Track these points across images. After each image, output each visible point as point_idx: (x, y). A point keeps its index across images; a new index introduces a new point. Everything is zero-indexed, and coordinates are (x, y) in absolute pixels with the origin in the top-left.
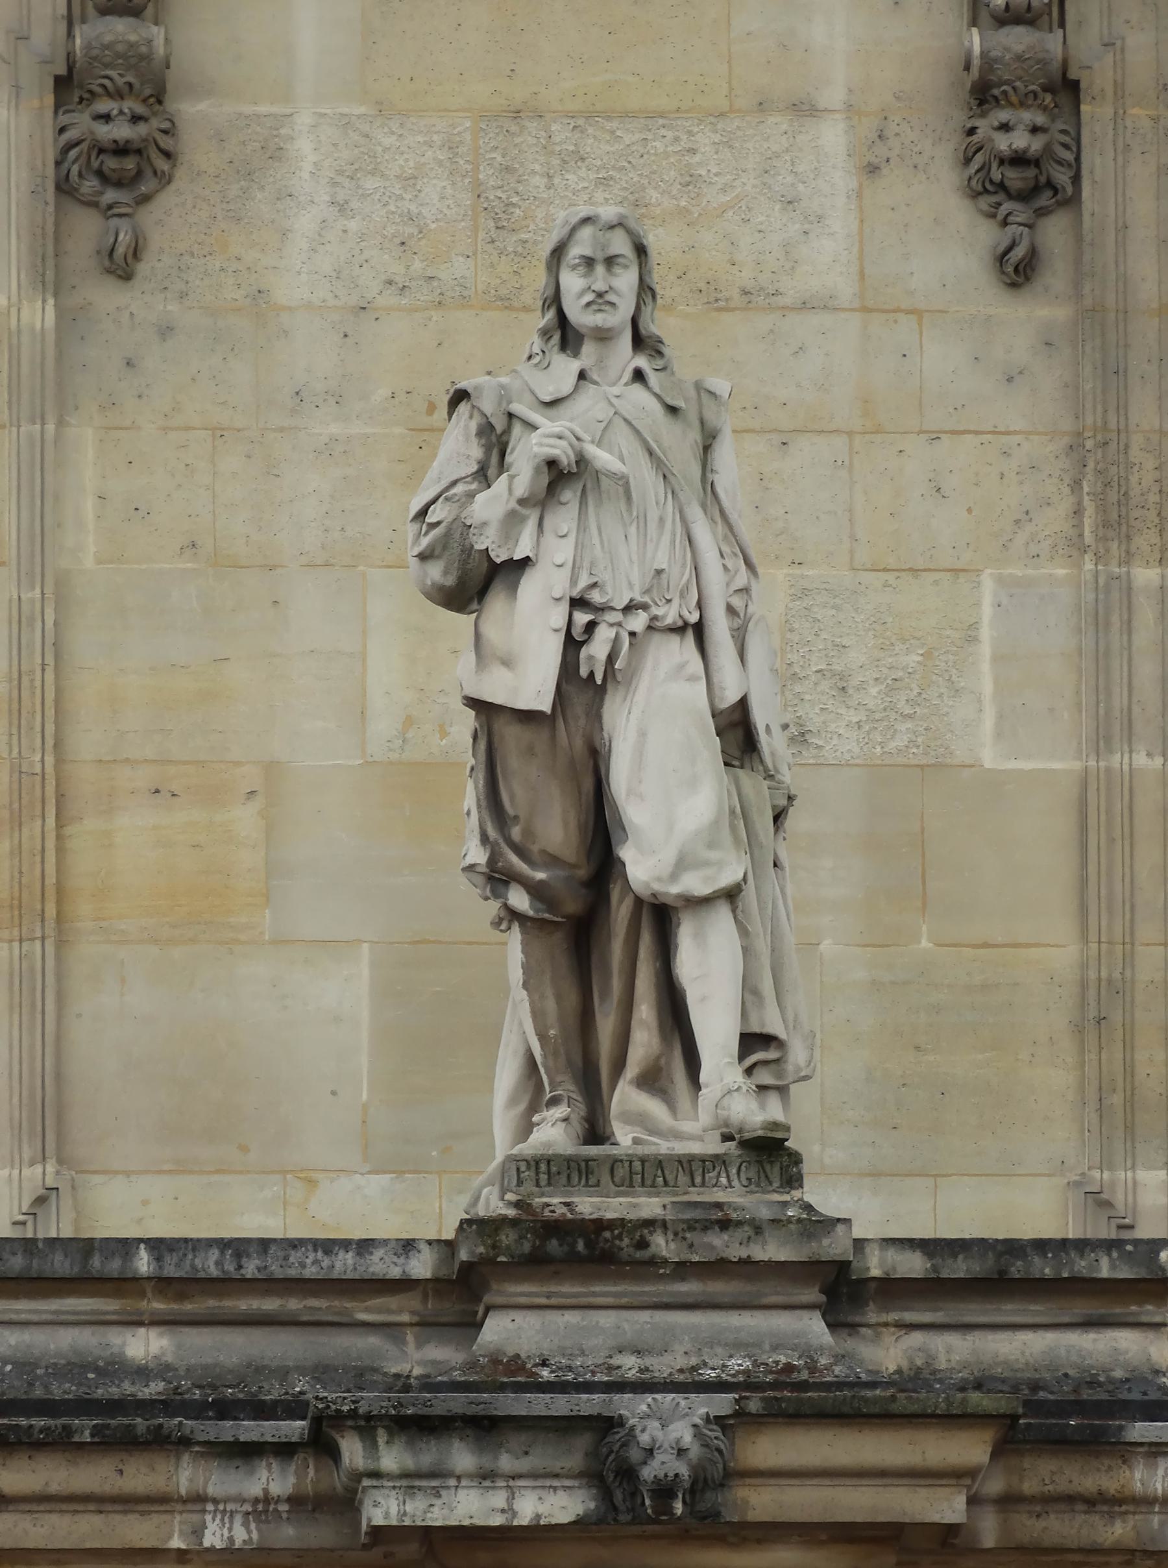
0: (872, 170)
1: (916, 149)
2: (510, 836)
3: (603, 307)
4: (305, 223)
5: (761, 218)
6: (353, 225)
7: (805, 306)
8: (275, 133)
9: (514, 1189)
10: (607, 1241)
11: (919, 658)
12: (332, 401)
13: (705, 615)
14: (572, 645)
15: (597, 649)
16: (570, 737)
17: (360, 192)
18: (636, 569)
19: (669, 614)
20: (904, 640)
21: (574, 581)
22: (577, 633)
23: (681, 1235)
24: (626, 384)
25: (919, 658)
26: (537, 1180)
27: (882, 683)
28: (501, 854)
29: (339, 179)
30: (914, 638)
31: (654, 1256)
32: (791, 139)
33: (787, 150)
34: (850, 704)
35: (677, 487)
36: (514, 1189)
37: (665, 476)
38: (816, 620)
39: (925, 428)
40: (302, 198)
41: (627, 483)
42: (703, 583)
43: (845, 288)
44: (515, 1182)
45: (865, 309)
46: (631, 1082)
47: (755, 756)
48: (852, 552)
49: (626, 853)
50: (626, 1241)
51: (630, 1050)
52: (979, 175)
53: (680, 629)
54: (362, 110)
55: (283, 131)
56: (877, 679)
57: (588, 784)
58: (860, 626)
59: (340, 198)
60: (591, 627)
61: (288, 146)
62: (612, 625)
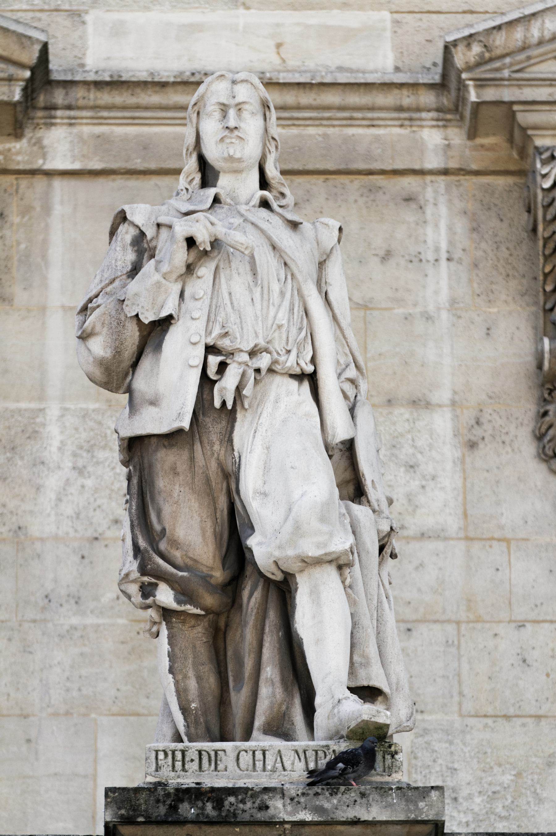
0: (472, 445)
1: (504, 431)
2: (158, 548)
3: (233, 140)
4: (52, 482)
5: (392, 477)
6: (89, 483)
7: (423, 536)
8: (32, 421)
9: (153, 774)
10: (231, 804)
11: (513, 778)
12: (72, 601)
13: (318, 369)
14: (206, 382)
15: (227, 385)
16: (208, 456)
17: (95, 460)
18: (260, 323)
19: (290, 362)
20: (500, 765)
21: (208, 332)
22: (212, 372)
23: (296, 800)
24: (254, 206)
25: (513, 778)
26: (173, 766)
27: (484, 795)
28: (150, 559)
29: (79, 452)
30: (508, 763)
31: (273, 817)
32: (412, 425)
33: (409, 432)
34: (460, 809)
35: (296, 271)
36: (153, 774)
37: (285, 264)
38: (434, 751)
39: (513, 618)
40: (51, 465)
41: (252, 257)
42: (317, 344)
43: (453, 523)
44: (154, 767)
45: (468, 538)
46: (259, 729)
47: (363, 499)
48: (460, 704)
49: (252, 542)
50: (249, 805)
51: (258, 704)
52: (551, 444)
53: (300, 377)
54: (97, 405)
55: (38, 420)
56: (480, 792)
57: (222, 503)
58: (467, 755)
59: (80, 464)
60: (222, 367)
61: (41, 430)
62: (240, 363)
